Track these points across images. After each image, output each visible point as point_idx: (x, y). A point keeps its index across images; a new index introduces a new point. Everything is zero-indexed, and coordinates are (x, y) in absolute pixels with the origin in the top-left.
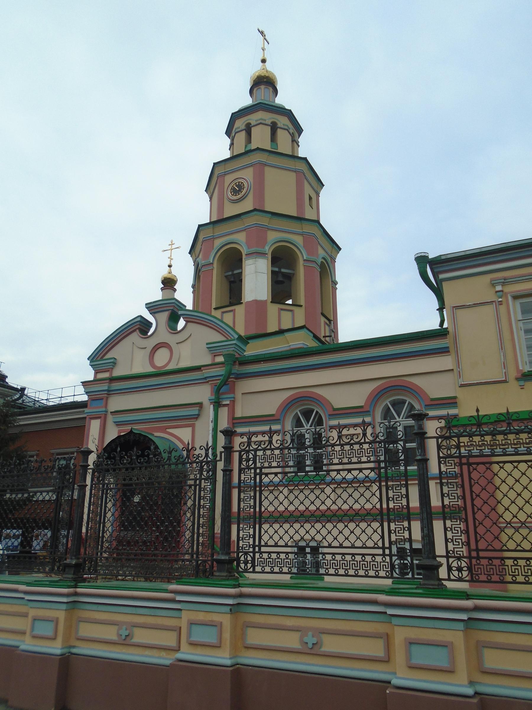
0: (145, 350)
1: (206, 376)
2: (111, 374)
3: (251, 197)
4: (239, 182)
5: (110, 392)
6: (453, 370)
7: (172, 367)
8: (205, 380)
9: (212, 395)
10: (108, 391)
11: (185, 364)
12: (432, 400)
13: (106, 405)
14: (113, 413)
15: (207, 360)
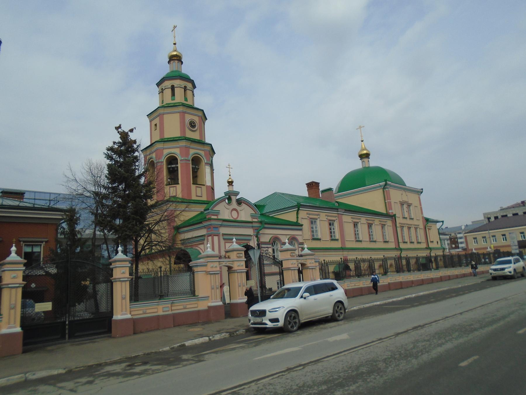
0: (228, 210)
1: (254, 226)
2: (217, 217)
3: (197, 133)
4: (193, 122)
5: (221, 226)
6: (301, 235)
7: (239, 219)
8: (252, 227)
9: (254, 233)
10: (221, 225)
11: (243, 219)
12: (300, 242)
13: (219, 231)
14: (223, 235)
15: (250, 219)
